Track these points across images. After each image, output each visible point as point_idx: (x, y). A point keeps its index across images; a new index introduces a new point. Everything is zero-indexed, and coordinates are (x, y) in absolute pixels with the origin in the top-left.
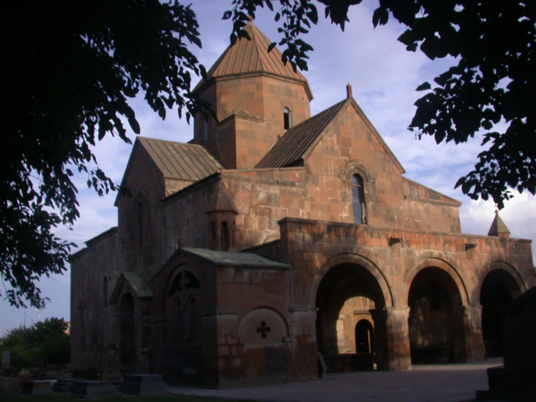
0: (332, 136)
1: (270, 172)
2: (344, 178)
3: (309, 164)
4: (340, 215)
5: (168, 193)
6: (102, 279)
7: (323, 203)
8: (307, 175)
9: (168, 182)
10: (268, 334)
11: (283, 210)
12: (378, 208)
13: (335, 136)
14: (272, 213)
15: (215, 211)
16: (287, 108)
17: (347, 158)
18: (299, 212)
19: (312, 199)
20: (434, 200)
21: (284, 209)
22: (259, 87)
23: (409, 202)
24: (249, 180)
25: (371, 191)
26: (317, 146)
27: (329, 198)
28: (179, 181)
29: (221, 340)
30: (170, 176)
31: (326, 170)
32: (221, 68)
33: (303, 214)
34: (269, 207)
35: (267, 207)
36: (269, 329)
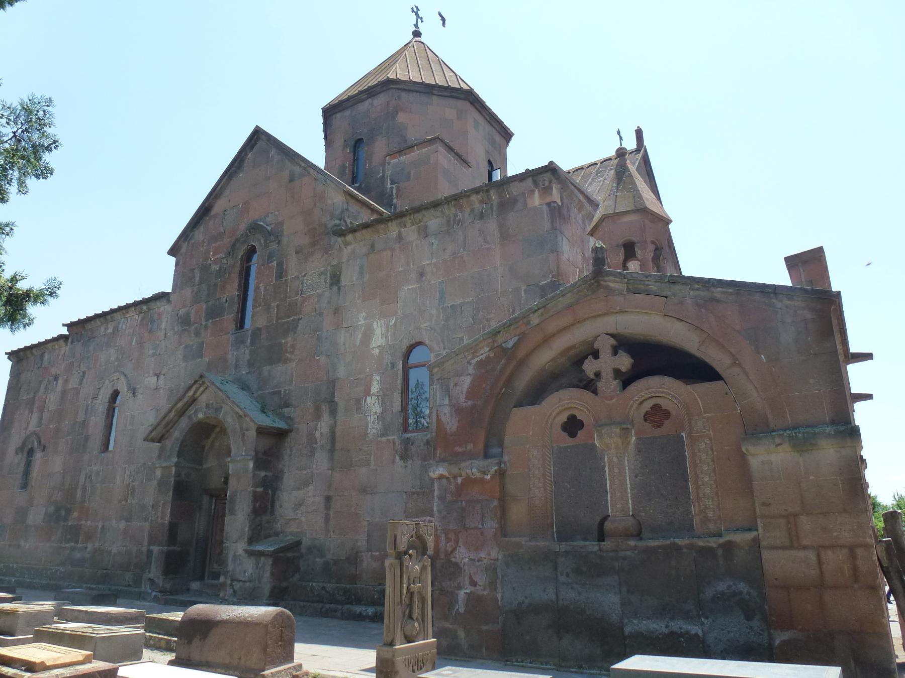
6: (105, 395)
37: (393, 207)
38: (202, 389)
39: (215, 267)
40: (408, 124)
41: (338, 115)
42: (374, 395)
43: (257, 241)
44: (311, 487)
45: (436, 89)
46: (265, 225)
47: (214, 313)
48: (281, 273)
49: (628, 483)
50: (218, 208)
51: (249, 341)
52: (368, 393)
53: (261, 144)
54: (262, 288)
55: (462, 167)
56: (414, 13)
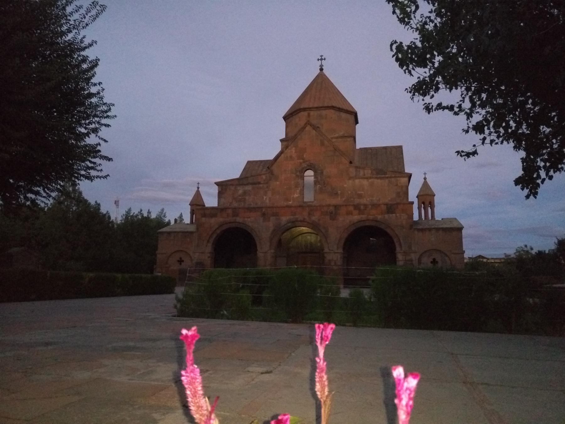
2: (298, 174)
4: (292, 196)
10: (182, 263)
12: (324, 188)
13: (294, 148)
17: (302, 161)
18: (263, 198)
20: (379, 176)
23: (353, 181)
24: (232, 185)
25: (319, 178)
26: (280, 158)
27: (285, 187)
33: (266, 199)
34: (244, 197)
35: (243, 197)
36: (183, 261)
56: (320, 60)
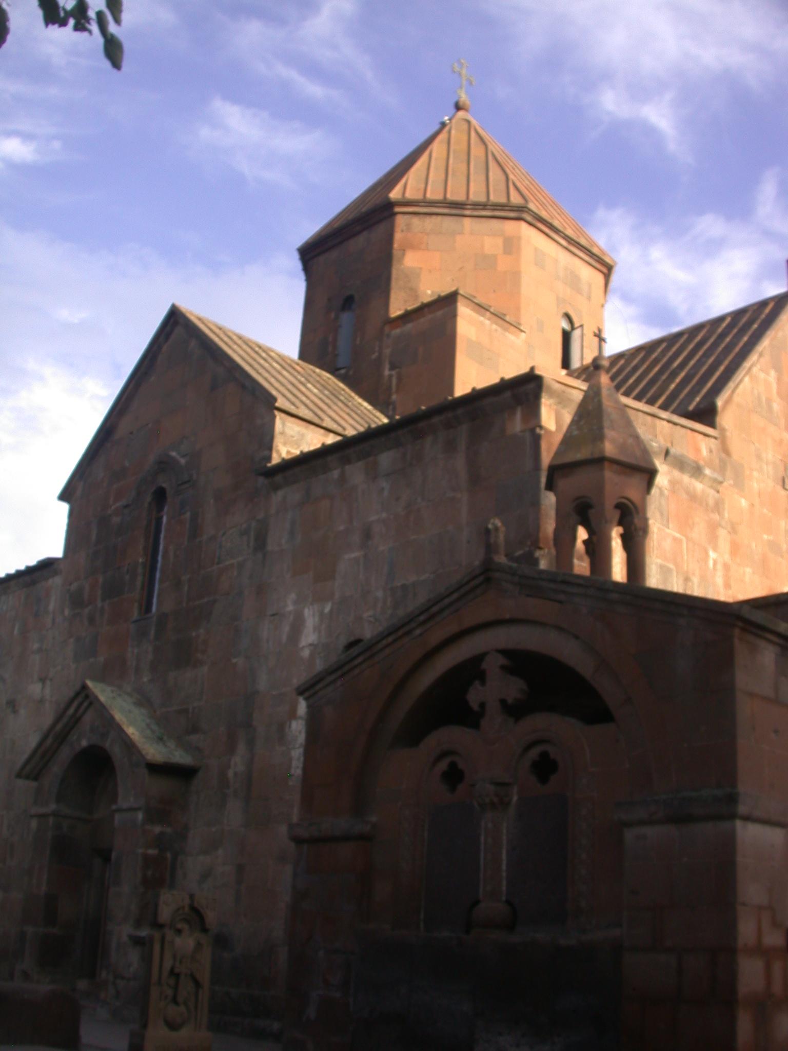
0: (768, 374)
1: (649, 418)
3: (727, 427)
5: (278, 452)
7: (754, 545)
8: (724, 455)
9: (284, 424)
11: (675, 539)
13: (773, 373)
14: (653, 541)
15: (600, 461)
16: (568, 317)
19: (734, 530)
21: (678, 535)
22: (511, 246)
28: (312, 427)
29: (746, 930)
30: (292, 409)
31: (759, 457)
32: (410, 182)
37: (391, 407)
38: (85, 704)
39: (116, 520)
40: (421, 268)
41: (322, 259)
42: (300, 718)
43: (163, 482)
44: (220, 852)
45: (469, 207)
46: (178, 457)
47: (113, 590)
48: (195, 531)
49: (504, 856)
50: (122, 430)
51: (152, 632)
52: (293, 715)
53: (179, 331)
54: (171, 554)
55: (507, 334)
